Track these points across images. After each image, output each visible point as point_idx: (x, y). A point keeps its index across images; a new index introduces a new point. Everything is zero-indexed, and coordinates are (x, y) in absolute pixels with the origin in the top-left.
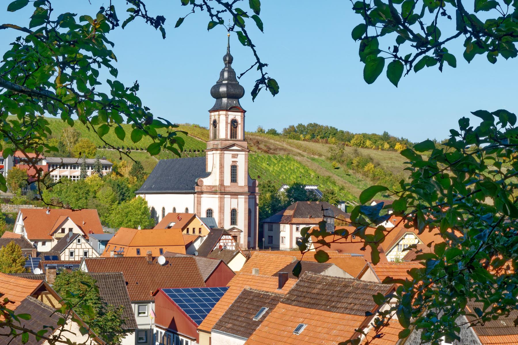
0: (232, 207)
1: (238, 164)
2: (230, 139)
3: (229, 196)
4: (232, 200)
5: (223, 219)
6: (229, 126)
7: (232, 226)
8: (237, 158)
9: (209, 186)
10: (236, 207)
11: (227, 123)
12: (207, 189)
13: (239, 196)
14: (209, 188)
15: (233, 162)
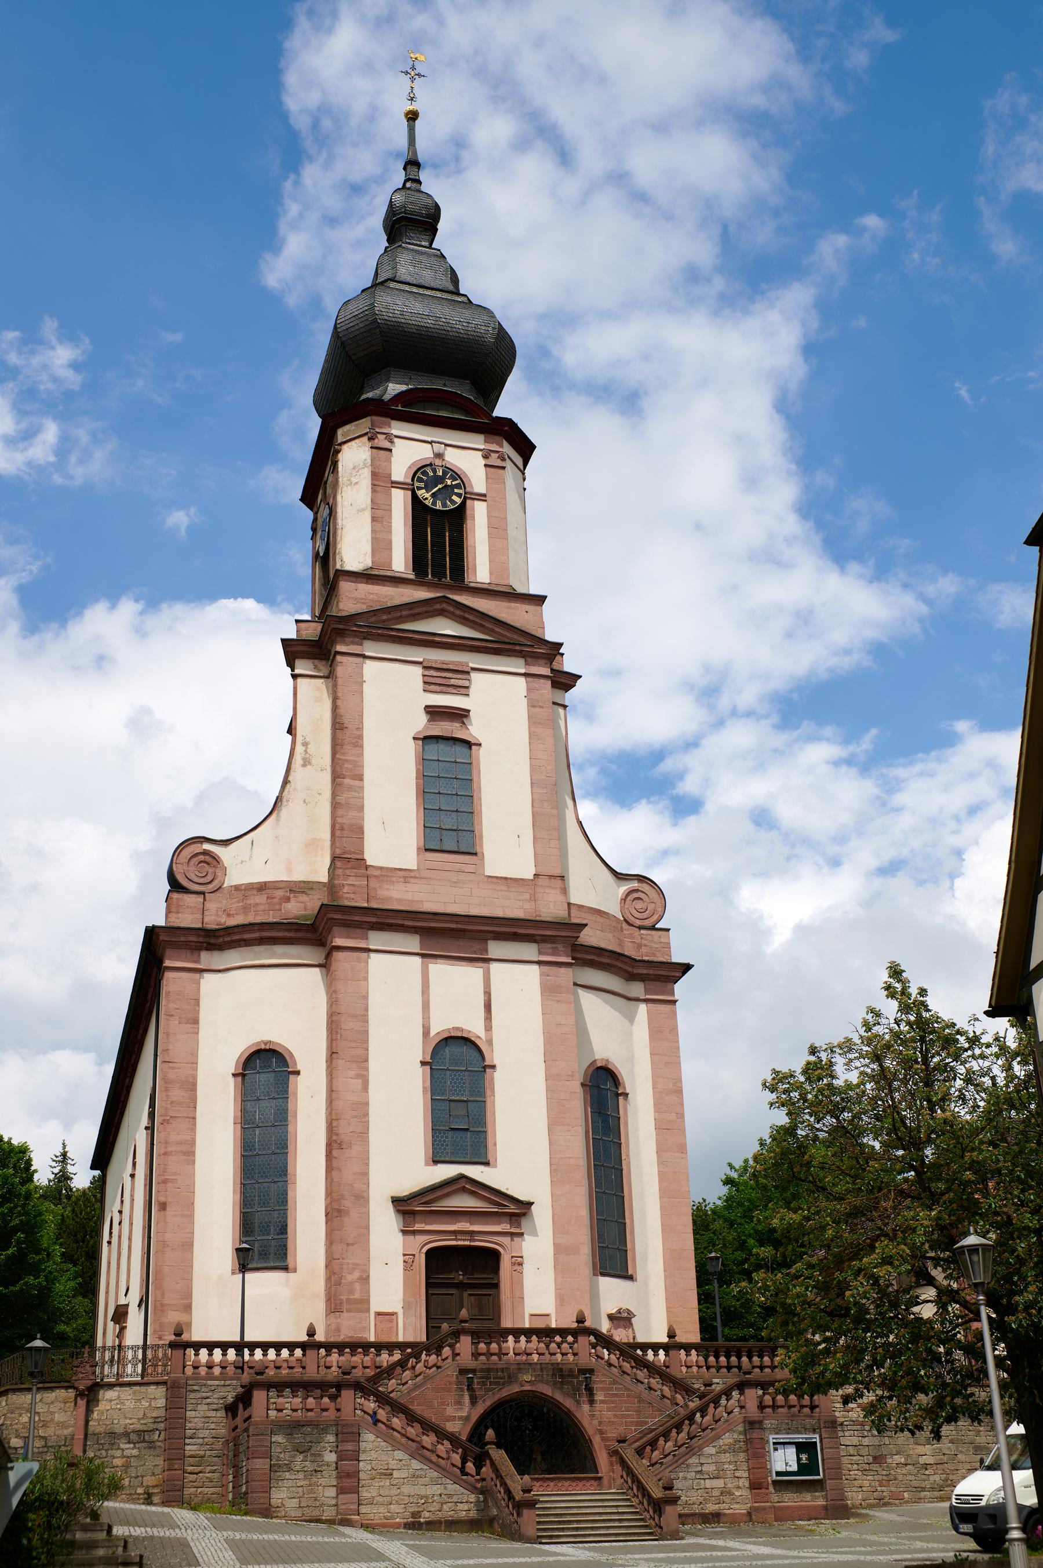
0: (439, 1026)
1: (475, 730)
2: (412, 577)
3: (413, 943)
4: (439, 970)
5: (362, 1109)
6: (400, 503)
7: (447, 1171)
8: (463, 690)
9: (262, 887)
10: (475, 1027)
11: (381, 481)
12: (246, 909)
13: (495, 949)
14: (260, 899)
15: (434, 713)
